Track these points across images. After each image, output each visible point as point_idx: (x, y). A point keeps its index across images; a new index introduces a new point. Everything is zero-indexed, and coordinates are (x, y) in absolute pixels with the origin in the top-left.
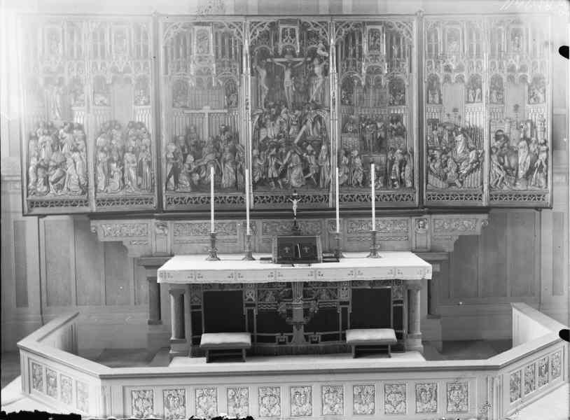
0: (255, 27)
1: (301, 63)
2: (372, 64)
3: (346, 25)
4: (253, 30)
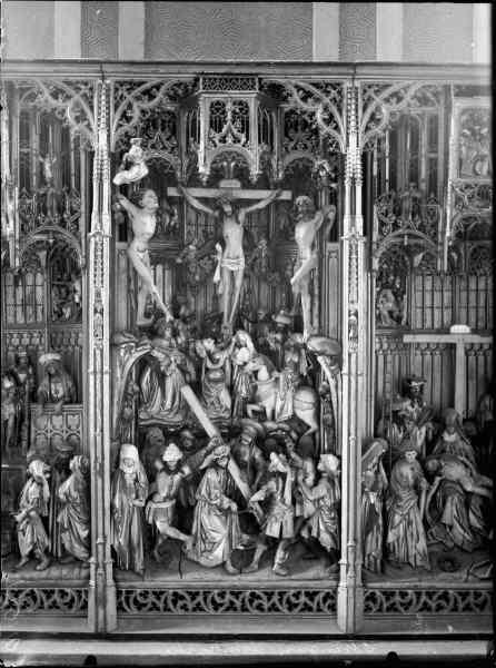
0: (129, 98)
1: (262, 205)
4: (121, 109)
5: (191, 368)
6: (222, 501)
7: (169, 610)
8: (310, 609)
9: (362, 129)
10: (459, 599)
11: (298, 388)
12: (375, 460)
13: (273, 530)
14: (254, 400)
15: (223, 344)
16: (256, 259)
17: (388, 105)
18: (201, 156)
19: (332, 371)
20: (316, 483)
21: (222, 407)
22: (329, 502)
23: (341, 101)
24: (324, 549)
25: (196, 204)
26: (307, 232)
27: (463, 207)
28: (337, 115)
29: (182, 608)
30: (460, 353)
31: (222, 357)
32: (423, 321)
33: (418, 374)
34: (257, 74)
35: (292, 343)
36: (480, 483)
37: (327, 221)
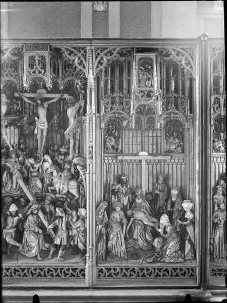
1: (55, 100)
2: (143, 102)
3: (109, 52)
5: (25, 172)
6: (35, 228)
7: (12, 276)
8: (74, 276)
9: (95, 67)
10: (140, 271)
11: (70, 179)
12: (102, 211)
13: (57, 242)
14: (51, 185)
15: (39, 161)
16: (52, 126)
17: (106, 57)
18: (25, 79)
19: (83, 172)
20: (77, 220)
21: (37, 188)
22: (82, 229)
23: (86, 55)
24: (80, 249)
25: (26, 100)
26: (71, 112)
27: (139, 100)
28: (84, 61)
29: (18, 275)
30: (144, 163)
31: (37, 166)
32: (129, 150)
33: (126, 173)
34: (49, 44)
35: (67, 160)
36: (151, 221)
37: (80, 107)
